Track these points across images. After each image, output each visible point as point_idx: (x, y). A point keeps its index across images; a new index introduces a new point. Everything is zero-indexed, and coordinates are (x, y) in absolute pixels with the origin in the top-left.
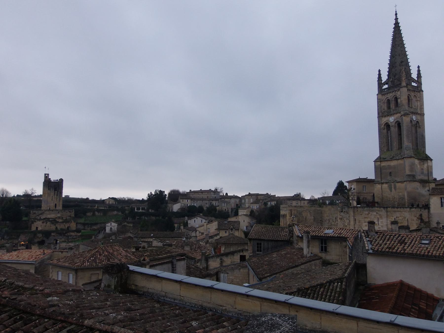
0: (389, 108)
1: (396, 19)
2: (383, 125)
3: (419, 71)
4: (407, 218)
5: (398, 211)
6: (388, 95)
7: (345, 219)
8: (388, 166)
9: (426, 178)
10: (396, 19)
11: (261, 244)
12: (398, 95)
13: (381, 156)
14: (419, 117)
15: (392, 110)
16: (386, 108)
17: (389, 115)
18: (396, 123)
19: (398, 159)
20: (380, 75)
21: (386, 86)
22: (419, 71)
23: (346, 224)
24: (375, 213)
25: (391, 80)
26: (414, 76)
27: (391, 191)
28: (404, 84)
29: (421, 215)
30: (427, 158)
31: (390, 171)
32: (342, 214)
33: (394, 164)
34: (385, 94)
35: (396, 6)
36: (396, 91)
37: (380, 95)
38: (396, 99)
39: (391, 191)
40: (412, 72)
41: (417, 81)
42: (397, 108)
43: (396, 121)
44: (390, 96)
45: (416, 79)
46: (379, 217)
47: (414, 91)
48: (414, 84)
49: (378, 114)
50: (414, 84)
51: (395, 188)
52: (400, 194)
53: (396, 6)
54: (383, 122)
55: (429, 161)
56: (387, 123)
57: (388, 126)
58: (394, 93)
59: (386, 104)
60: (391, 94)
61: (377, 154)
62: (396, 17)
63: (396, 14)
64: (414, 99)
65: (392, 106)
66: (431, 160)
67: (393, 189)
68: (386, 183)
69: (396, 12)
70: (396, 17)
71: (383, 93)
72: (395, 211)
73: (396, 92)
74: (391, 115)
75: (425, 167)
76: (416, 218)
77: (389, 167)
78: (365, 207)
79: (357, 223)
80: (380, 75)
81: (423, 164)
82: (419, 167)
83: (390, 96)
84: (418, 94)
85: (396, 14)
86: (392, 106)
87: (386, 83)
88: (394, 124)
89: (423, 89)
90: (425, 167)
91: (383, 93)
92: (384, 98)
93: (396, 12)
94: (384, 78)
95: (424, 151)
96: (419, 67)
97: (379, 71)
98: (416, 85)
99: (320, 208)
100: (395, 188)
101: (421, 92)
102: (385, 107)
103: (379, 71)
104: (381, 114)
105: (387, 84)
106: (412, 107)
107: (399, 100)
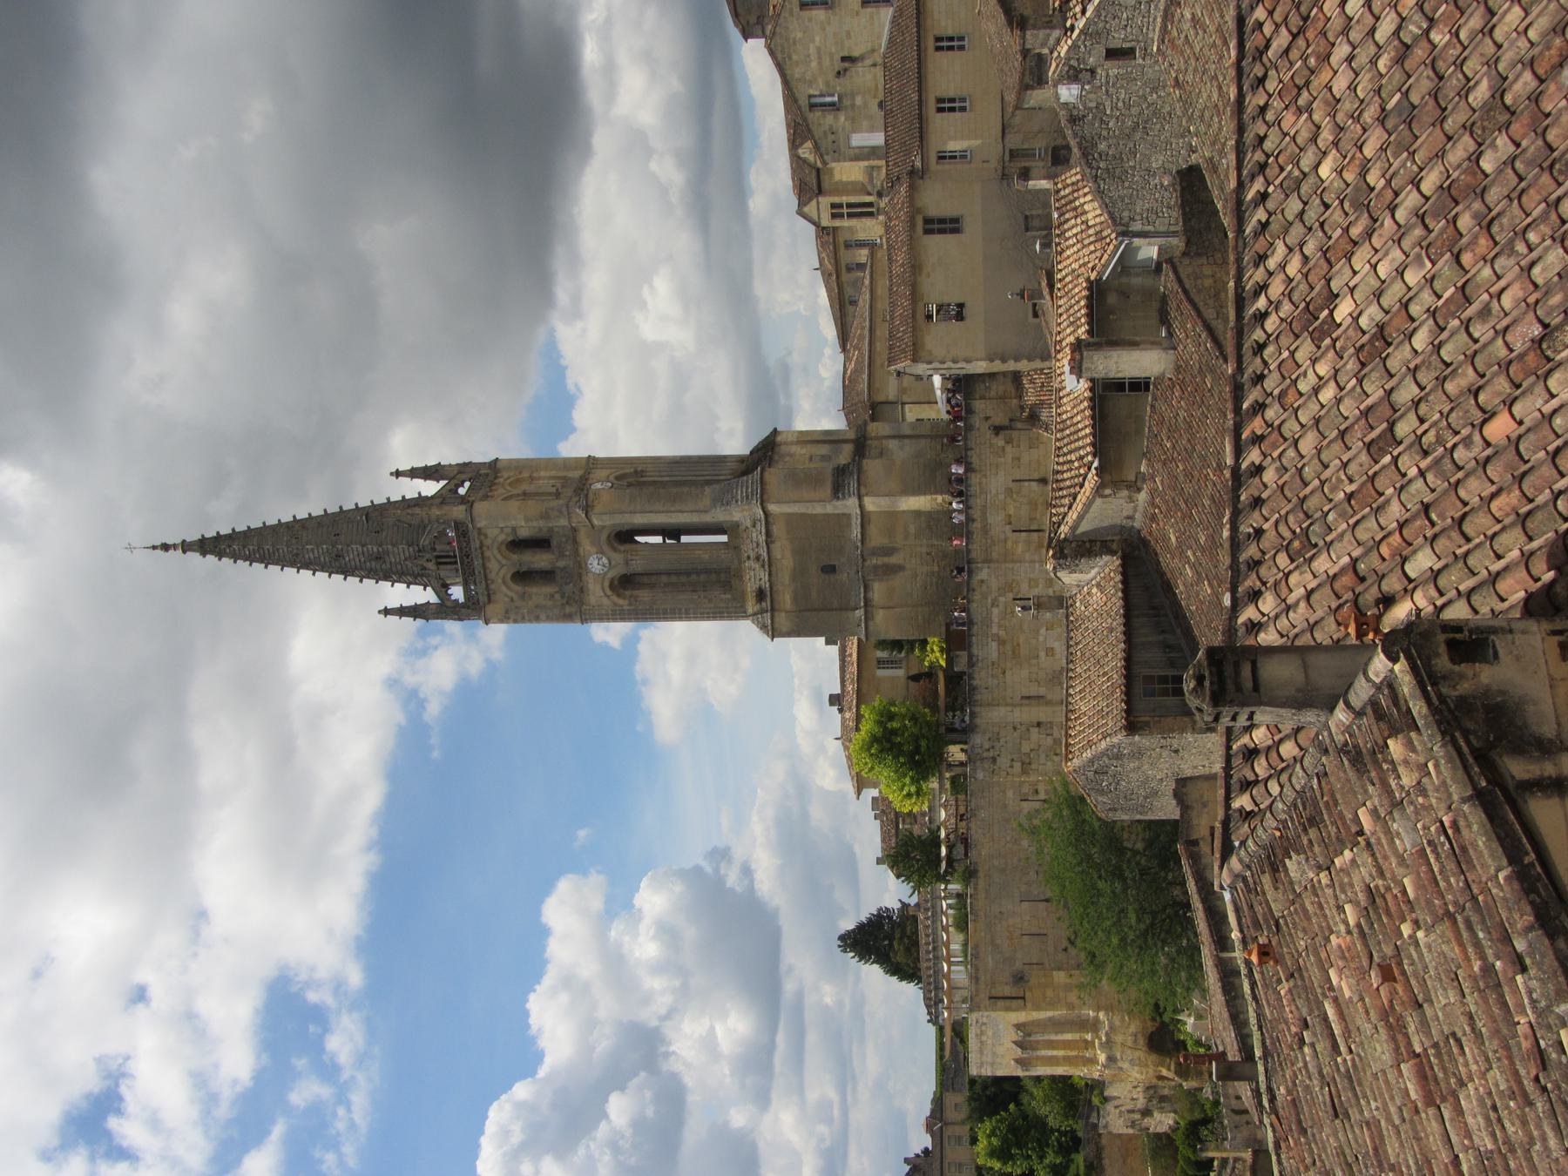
0: (547, 576)
1: (186, 547)
2: (621, 602)
3: (414, 473)
4: (1011, 485)
5: (984, 518)
6: (492, 576)
7: (1026, 747)
8: (794, 578)
10: (186, 547)
11: (1149, 679)
12: (502, 538)
13: (750, 611)
15: (561, 564)
16: (548, 589)
17: (578, 571)
18: (615, 550)
19: (768, 534)
20: (402, 612)
21: (457, 593)
22: (414, 473)
23: (1050, 740)
24: (995, 611)
25: (431, 566)
26: (430, 488)
27: (901, 568)
28: (458, 512)
32: (1003, 762)
33: (788, 554)
34: (487, 588)
35: (131, 548)
36: (481, 546)
37: (490, 609)
38: (518, 544)
39: (899, 568)
42: (554, 543)
43: (606, 548)
44: (499, 567)
45: (443, 483)
46: (1011, 596)
47: (492, 484)
49: (568, 618)
51: (888, 551)
52: (912, 529)
53: (131, 548)
54: (606, 601)
55: (779, 439)
56: (611, 587)
57: (625, 583)
58: (487, 554)
59: (534, 590)
60: (493, 566)
61: (746, 631)
62: (175, 547)
63: (165, 547)
65: (541, 560)
66: (775, 432)
67: (894, 560)
68: (866, 588)
69: (154, 548)
70: (175, 547)
71: (483, 599)
73: (488, 542)
74: (580, 567)
76: (1009, 449)
77: (799, 573)
78: (970, 656)
79: (1042, 691)
80: (402, 612)
83: (499, 567)
84: (505, 475)
85: (165, 547)
86: (541, 560)
87: (442, 588)
88: (618, 558)
91: (483, 599)
92: (505, 591)
93: (154, 548)
94: (422, 595)
97: (386, 612)
98: (467, 484)
99: (981, 874)
101: (499, 465)
102: (540, 593)
103: (386, 612)
104: (568, 610)
105: (446, 586)
107: (524, 533)
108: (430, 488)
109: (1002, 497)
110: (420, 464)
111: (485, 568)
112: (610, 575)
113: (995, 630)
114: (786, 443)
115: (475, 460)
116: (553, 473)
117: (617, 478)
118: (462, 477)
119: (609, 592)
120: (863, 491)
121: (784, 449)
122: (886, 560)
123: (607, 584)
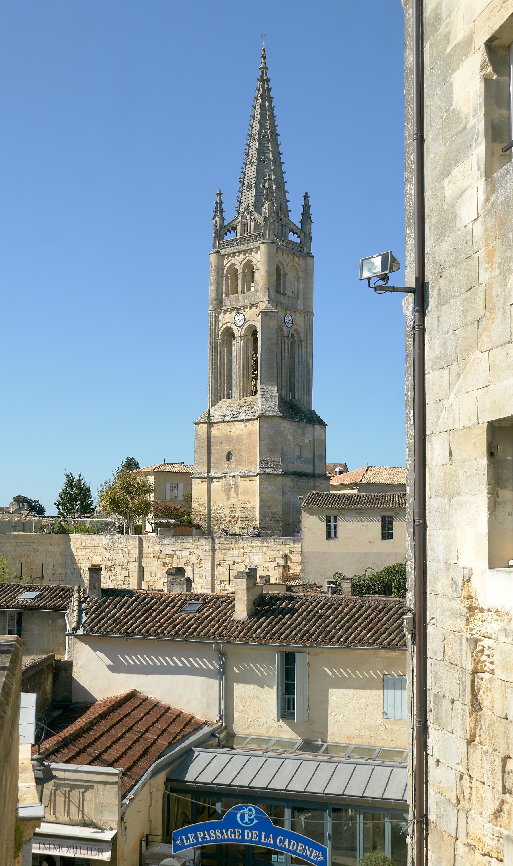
3: (306, 206)
9: (308, 469)
12: (255, 262)
14: (300, 319)
22: (306, 206)
24: (188, 553)
26: (295, 217)
29: (286, 557)
30: (315, 420)
31: (229, 447)
33: (238, 433)
36: (251, 250)
40: (290, 206)
41: (302, 230)
43: (247, 324)
45: (299, 226)
48: (292, 237)
50: (292, 237)
51: (236, 491)
52: (247, 505)
53: (264, 36)
55: (317, 427)
64: (291, 275)
66: (323, 424)
67: (232, 493)
72: (232, 549)
75: (307, 442)
81: (303, 434)
82: (291, 440)
84: (302, 262)
89: (313, 253)
90: (307, 442)
95: (309, 402)
96: (306, 197)
98: (298, 241)
100: (236, 491)
101: (309, 258)
106: (284, 295)
108: (295, 217)
109: (248, 559)
110: (311, 211)
111: (239, 252)
112: (234, 328)
113: (178, 553)
114: (314, 432)
115: (312, 244)
116: (301, 291)
117: (296, 330)
118: (302, 235)
119: (224, 327)
120: (262, 476)
121: (309, 429)
122: (233, 490)
123: (229, 325)
